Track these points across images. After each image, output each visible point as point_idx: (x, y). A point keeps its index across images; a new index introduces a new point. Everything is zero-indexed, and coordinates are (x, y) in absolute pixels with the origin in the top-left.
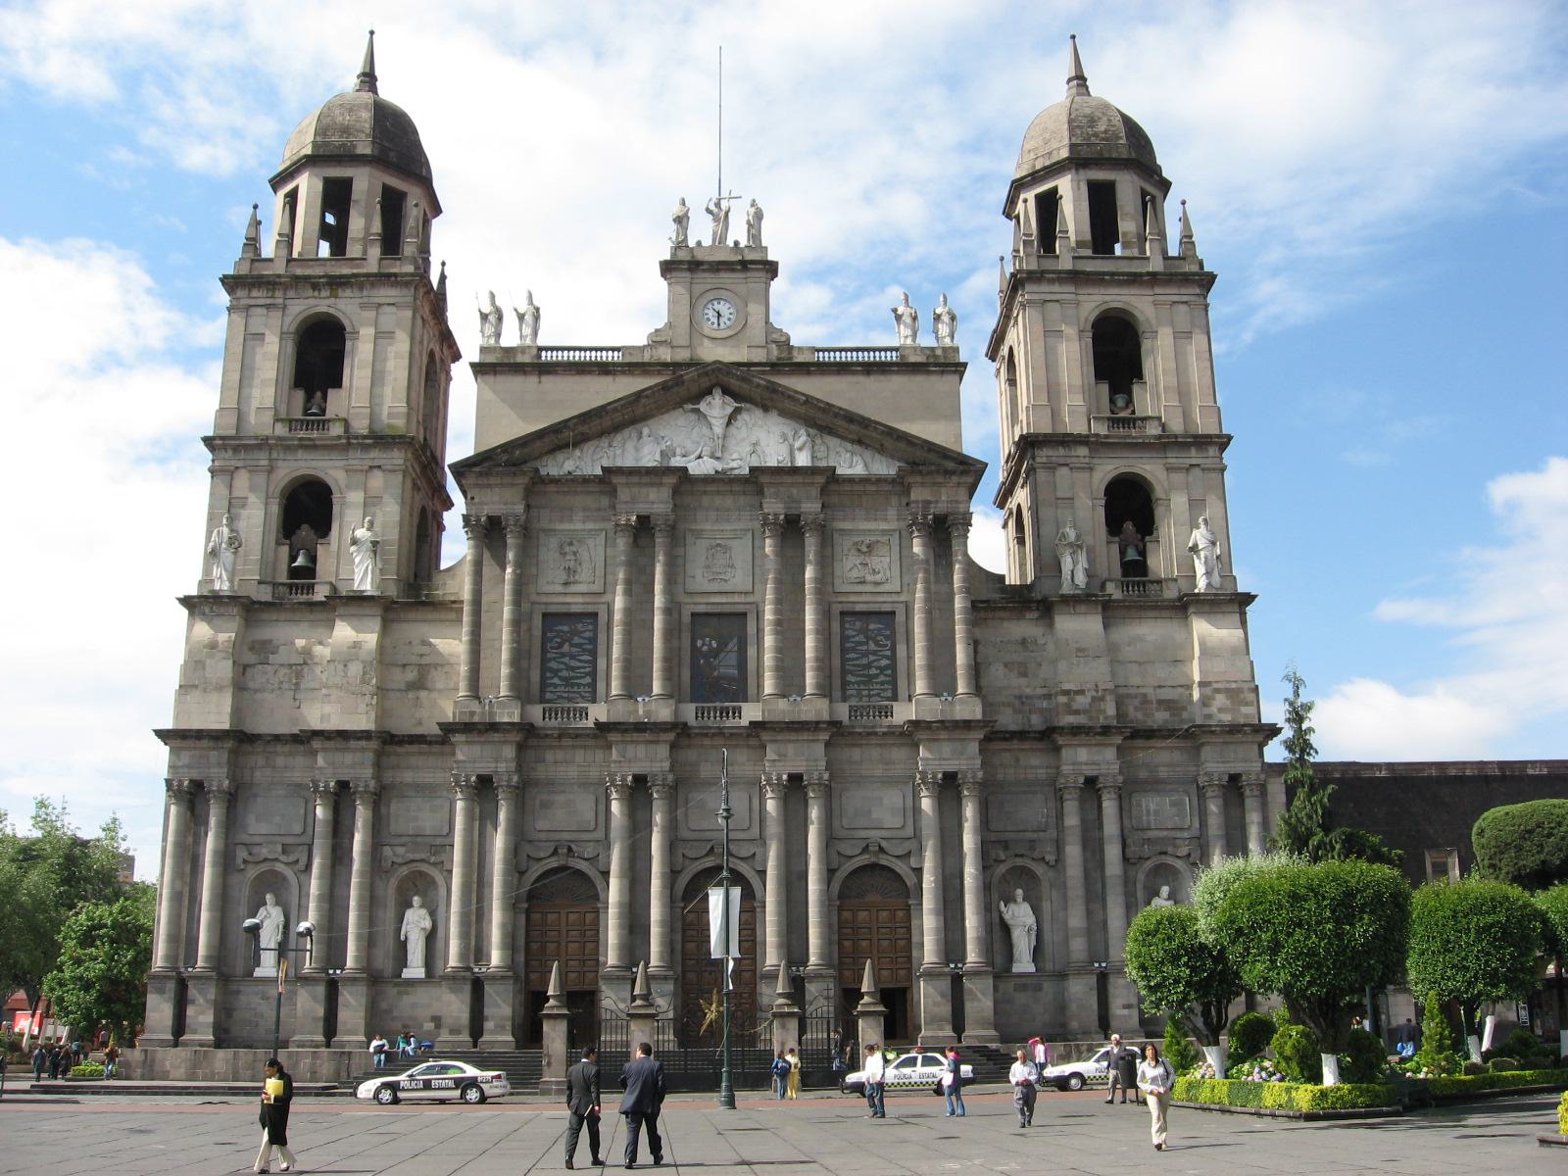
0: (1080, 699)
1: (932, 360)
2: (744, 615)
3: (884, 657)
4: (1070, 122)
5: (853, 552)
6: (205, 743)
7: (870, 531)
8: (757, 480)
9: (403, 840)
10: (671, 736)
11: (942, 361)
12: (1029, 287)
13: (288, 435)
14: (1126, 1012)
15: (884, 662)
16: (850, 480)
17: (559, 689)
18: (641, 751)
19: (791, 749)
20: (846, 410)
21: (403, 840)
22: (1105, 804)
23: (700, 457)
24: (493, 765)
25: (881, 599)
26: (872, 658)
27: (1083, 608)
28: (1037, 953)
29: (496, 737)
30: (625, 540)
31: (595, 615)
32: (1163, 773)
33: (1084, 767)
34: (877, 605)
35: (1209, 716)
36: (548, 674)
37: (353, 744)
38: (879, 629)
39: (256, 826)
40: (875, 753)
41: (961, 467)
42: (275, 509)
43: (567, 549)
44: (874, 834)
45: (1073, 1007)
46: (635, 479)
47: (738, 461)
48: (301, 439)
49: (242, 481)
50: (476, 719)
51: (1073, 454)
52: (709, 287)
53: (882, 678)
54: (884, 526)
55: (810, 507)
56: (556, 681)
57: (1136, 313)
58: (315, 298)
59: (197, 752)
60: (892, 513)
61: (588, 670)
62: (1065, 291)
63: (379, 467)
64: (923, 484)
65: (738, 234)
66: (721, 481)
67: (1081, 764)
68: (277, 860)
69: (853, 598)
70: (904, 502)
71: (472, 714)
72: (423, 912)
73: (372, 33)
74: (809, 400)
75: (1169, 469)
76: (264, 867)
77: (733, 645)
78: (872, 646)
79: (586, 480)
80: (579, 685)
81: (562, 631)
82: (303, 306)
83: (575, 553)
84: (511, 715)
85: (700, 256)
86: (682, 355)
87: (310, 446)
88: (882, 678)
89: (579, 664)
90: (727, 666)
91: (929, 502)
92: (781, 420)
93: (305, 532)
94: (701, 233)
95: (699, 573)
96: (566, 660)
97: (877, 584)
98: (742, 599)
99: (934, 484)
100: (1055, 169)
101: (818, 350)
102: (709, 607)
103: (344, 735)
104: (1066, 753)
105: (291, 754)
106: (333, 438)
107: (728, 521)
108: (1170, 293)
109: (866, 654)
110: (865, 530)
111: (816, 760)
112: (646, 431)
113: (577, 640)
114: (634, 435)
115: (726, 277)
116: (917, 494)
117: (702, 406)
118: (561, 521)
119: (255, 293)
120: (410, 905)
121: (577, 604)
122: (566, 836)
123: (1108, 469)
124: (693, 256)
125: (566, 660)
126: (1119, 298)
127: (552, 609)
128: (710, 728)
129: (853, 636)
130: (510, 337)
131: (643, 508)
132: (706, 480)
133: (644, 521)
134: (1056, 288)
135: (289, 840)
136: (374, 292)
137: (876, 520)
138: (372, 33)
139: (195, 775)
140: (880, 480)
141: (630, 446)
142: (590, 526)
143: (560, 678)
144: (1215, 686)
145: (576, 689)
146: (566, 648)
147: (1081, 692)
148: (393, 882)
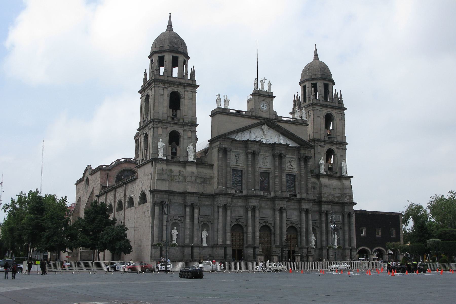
0: (325, 195)
1: (303, 122)
2: (269, 173)
3: (293, 184)
4: (320, 68)
5: (289, 162)
6: (164, 193)
7: (292, 157)
8: (274, 145)
9: (202, 216)
10: (260, 198)
11: (304, 123)
12: (314, 106)
13: (171, 120)
14: (332, 256)
15: (293, 185)
16: (290, 147)
17: (235, 186)
18: (254, 201)
19: (280, 202)
20: (291, 133)
21: (202, 216)
22: (328, 216)
23: (262, 139)
24: (227, 202)
25: (293, 172)
26: (291, 184)
27: (324, 176)
28: (315, 245)
29: (228, 196)
30: (250, 156)
31: (242, 171)
32: (337, 210)
33: (326, 209)
34: (293, 173)
35: (346, 200)
36: (233, 183)
37: (195, 195)
38: (292, 178)
39: (172, 212)
40: (292, 204)
41: (311, 147)
42: (168, 138)
43: (237, 156)
44: (292, 220)
45: (323, 255)
46: (252, 143)
47: (271, 141)
48: (174, 122)
49: (160, 131)
50: (224, 192)
51: (321, 143)
52: (262, 100)
53: (293, 188)
54: (294, 157)
55: (283, 152)
56: (234, 184)
57: (333, 115)
58: (174, 87)
59: (161, 195)
60: (296, 154)
61: (240, 182)
62: (320, 108)
63: (191, 131)
64: (303, 149)
65: (266, 88)
66: (266, 145)
67: (325, 208)
68: (177, 219)
69: (289, 172)
70: (298, 152)
71: (223, 191)
72: (206, 232)
73: (170, 14)
74: (285, 130)
75: (337, 148)
76: (174, 221)
77: (267, 179)
78: (291, 182)
80: (239, 185)
81: (234, 173)
82: (171, 89)
83: (238, 157)
84: (230, 192)
85: (260, 92)
86: (257, 115)
87: (175, 124)
88: (293, 188)
89: (239, 181)
90: (266, 184)
91: (304, 153)
92: (276, 132)
93: (174, 144)
94: (259, 87)
95: (261, 164)
96: (236, 180)
97: (293, 169)
98: (269, 170)
99: (305, 150)
100: (318, 79)
101: (283, 117)
102: (263, 171)
103: (193, 193)
104: (323, 206)
105: (179, 196)
106: (180, 123)
107: (267, 153)
108: (338, 111)
109: (290, 183)
110: (291, 157)
111: (285, 205)
112: (252, 131)
113: (238, 176)
114: (249, 132)
115: (265, 99)
116: (302, 151)
117: (263, 127)
118: (236, 149)
119: (160, 84)
120: (203, 230)
121: (239, 168)
122: (238, 217)
123: (327, 147)
124: (259, 93)
125: (236, 180)
126: (330, 111)
127: (234, 169)
128: (265, 197)
129: (288, 179)
130: (223, 106)
131: (254, 149)
132: (264, 144)
133: (254, 151)
134: (319, 107)
135: (179, 215)
136: (187, 88)
137: (293, 155)
138: (170, 14)
139: (161, 200)
140: (295, 147)
141: (248, 134)
142: (241, 151)
143: (235, 184)
144: (347, 194)
145: (238, 186)
146: (236, 177)
147: (325, 194)
148: (201, 225)
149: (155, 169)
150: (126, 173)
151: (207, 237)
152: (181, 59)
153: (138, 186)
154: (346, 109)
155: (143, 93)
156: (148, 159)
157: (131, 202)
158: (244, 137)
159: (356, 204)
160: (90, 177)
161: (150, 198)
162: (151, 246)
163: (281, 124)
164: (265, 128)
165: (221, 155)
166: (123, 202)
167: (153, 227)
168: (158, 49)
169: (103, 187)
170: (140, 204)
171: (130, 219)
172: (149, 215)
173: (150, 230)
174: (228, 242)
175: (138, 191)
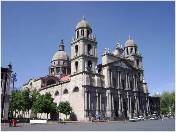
74: (129, 64)
79: (115, 66)
103: (100, 87)
149: (84, 76)
150: (51, 81)
151: (104, 107)
152: (90, 32)
153: (72, 84)
154: (142, 58)
155: (73, 45)
156: (79, 72)
157: (66, 91)
158: (116, 65)
159: (149, 94)
160: (33, 83)
161: (82, 89)
162: (84, 110)
163: (128, 62)
164: (122, 62)
165: (109, 72)
166: (60, 92)
167: (84, 102)
168: (81, 27)
169: (42, 86)
170: (73, 92)
171: (65, 99)
172: (82, 96)
173: (83, 103)
174: (113, 109)
175: (72, 86)
